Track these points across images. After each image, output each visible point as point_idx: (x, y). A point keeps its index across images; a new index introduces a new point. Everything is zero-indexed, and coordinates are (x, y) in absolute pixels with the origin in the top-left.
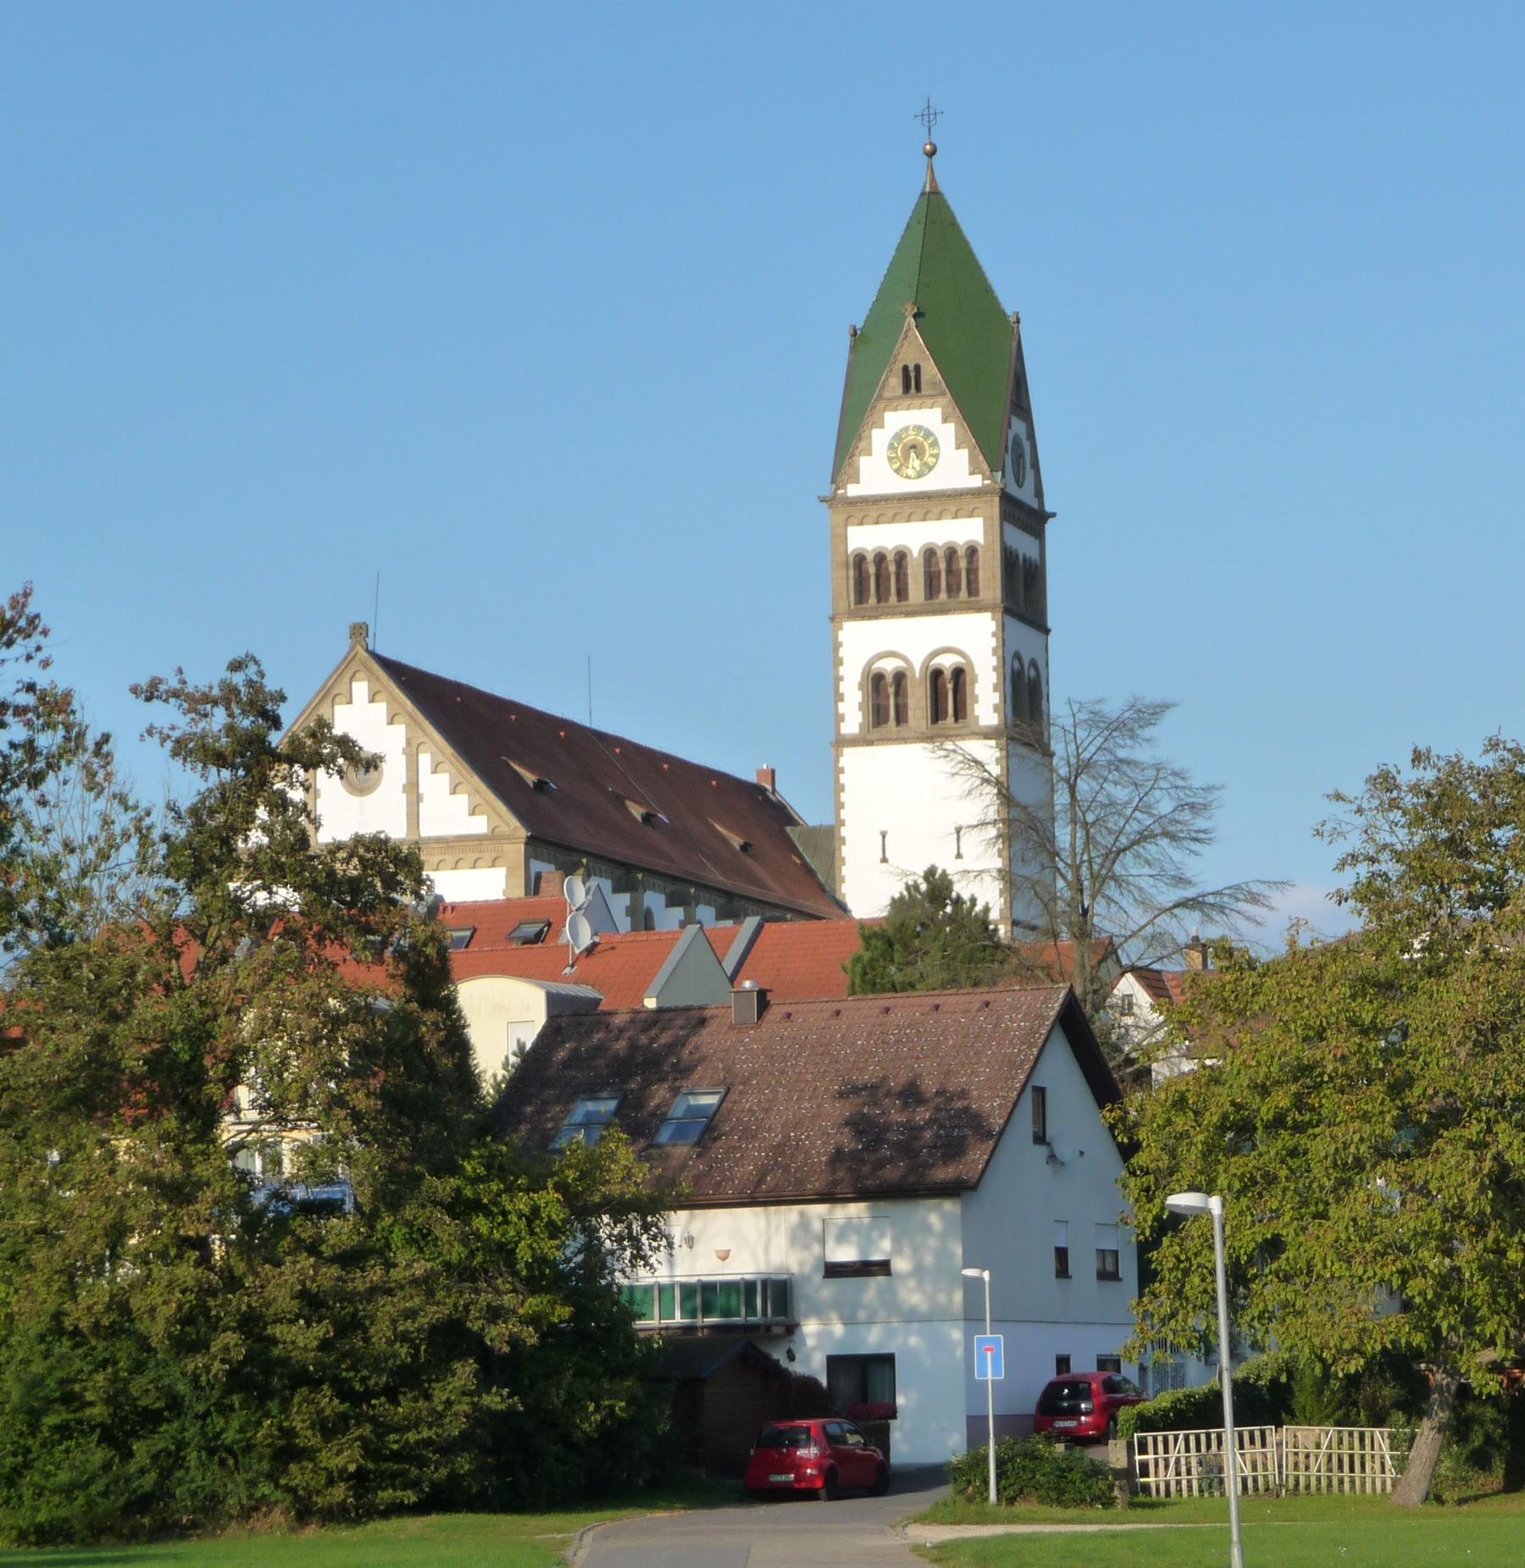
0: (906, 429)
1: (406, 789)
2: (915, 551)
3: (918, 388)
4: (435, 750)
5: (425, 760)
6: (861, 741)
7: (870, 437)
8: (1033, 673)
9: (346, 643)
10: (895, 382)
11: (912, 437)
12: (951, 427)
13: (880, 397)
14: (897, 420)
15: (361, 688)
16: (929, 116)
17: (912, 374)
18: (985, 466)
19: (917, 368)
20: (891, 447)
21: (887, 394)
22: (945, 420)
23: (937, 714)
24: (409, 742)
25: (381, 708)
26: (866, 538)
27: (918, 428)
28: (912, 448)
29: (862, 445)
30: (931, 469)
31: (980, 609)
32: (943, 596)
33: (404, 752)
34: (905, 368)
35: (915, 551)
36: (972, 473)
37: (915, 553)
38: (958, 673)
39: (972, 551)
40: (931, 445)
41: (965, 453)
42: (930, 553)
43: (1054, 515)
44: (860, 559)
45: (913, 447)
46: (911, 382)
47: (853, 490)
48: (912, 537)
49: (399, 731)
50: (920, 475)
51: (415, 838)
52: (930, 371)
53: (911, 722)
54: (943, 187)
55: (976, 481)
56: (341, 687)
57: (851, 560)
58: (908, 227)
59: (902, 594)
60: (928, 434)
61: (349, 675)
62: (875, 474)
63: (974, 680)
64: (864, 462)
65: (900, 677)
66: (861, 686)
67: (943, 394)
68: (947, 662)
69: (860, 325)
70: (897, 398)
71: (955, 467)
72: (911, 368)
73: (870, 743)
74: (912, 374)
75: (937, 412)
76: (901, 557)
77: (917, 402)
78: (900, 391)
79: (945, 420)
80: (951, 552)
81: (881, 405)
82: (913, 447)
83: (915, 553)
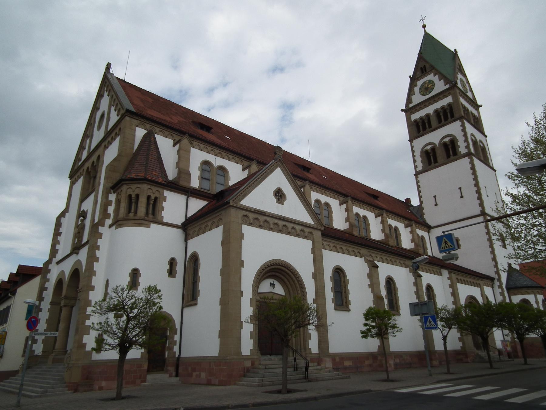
3: (426, 71)
6: (424, 171)
8: (482, 145)
16: (423, 19)
19: (425, 66)
20: (420, 89)
23: (448, 156)
26: (416, 116)
29: (412, 93)
34: (421, 68)
39: (450, 105)
41: (442, 81)
42: (436, 111)
43: (481, 106)
44: (416, 121)
48: (430, 110)
53: (439, 161)
55: (448, 86)
63: (457, 141)
64: (413, 97)
65: (433, 149)
66: (421, 156)
68: (447, 139)
71: (440, 86)
73: (426, 171)
75: (432, 74)
76: (428, 116)
78: (420, 75)
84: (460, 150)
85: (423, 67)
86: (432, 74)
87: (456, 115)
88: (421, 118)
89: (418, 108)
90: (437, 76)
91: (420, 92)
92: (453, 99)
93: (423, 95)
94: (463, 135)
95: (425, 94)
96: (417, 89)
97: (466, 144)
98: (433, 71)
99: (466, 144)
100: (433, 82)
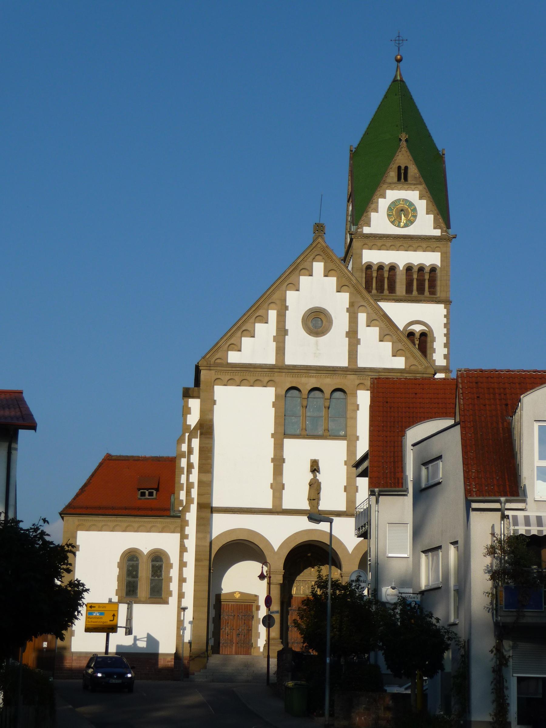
0: (399, 200)
1: (348, 334)
2: (401, 266)
3: (406, 179)
4: (370, 310)
5: (362, 317)
7: (377, 203)
9: (311, 236)
10: (392, 175)
11: (401, 205)
12: (424, 202)
13: (385, 182)
14: (393, 195)
15: (318, 267)
17: (402, 172)
18: (443, 225)
19: (406, 168)
20: (390, 209)
21: (389, 180)
22: (421, 198)
24: (352, 304)
25: (332, 281)
26: (372, 256)
27: (405, 201)
28: (401, 212)
29: (373, 206)
30: (412, 223)
31: (438, 302)
32: (415, 293)
33: (348, 310)
34: (399, 168)
35: (401, 266)
36: (435, 228)
37: (401, 269)
38: (423, 335)
39: (433, 269)
40: (412, 210)
41: (431, 217)
42: (409, 268)
44: (369, 267)
45: (402, 210)
46: (403, 177)
47: (366, 230)
48: (401, 258)
49: (345, 298)
50: (406, 226)
51: (353, 367)
52: (413, 170)
54: (404, 79)
55: (438, 233)
56: (306, 265)
57: (364, 267)
58: (386, 97)
59: (392, 289)
60: (411, 204)
61: (312, 257)
62: (379, 222)
63: (434, 340)
67: (420, 184)
68: (418, 328)
69: (355, 145)
70: (394, 183)
71: (425, 224)
72: (403, 167)
74: (402, 172)
75: (416, 193)
76: (393, 268)
77: (406, 186)
78: (396, 179)
79: (421, 198)
80: (421, 269)
81: (385, 186)
82: (402, 210)
83: (401, 269)
84: (435, 356)
85: (403, 167)
86: (416, 193)
87: (440, 293)
88: (381, 267)
89: (379, 243)
90: (424, 202)
91: (389, 215)
92: (442, 261)
93: (392, 222)
94: (445, 335)
95: (397, 223)
96: (383, 204)
97: (445, 351)
98: (421, 187)
99: (445, 351)
100: (415, 210)
